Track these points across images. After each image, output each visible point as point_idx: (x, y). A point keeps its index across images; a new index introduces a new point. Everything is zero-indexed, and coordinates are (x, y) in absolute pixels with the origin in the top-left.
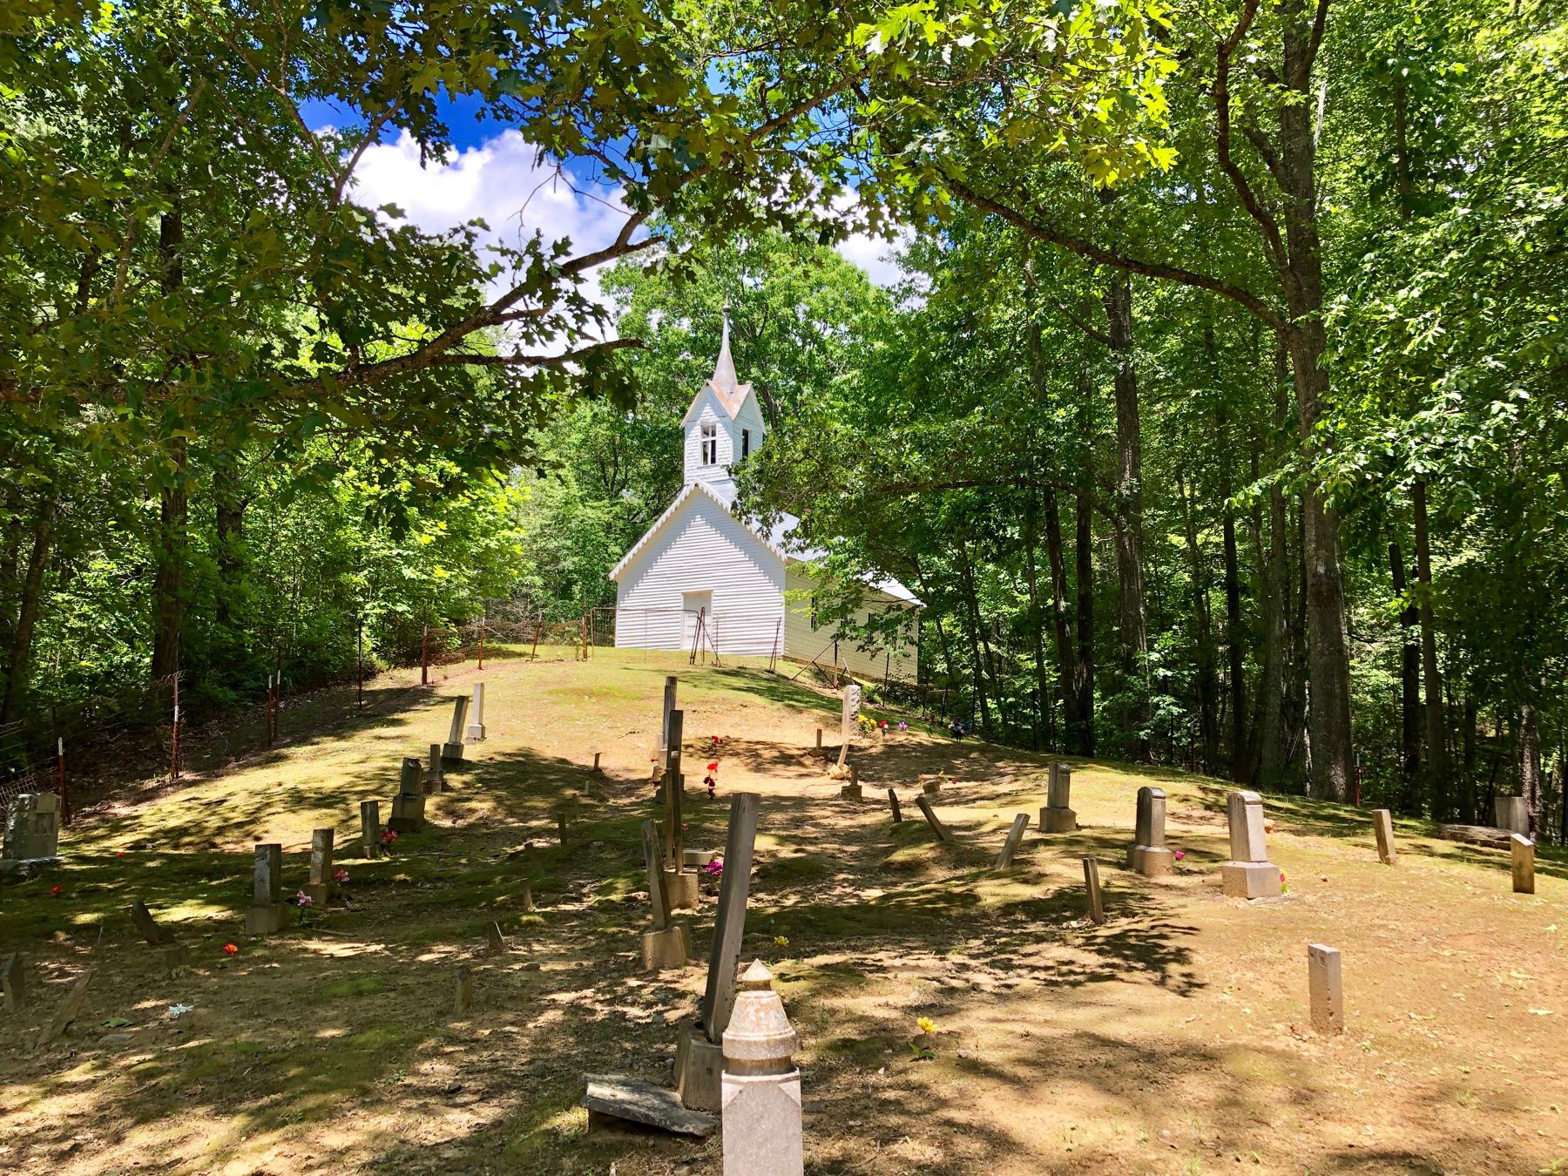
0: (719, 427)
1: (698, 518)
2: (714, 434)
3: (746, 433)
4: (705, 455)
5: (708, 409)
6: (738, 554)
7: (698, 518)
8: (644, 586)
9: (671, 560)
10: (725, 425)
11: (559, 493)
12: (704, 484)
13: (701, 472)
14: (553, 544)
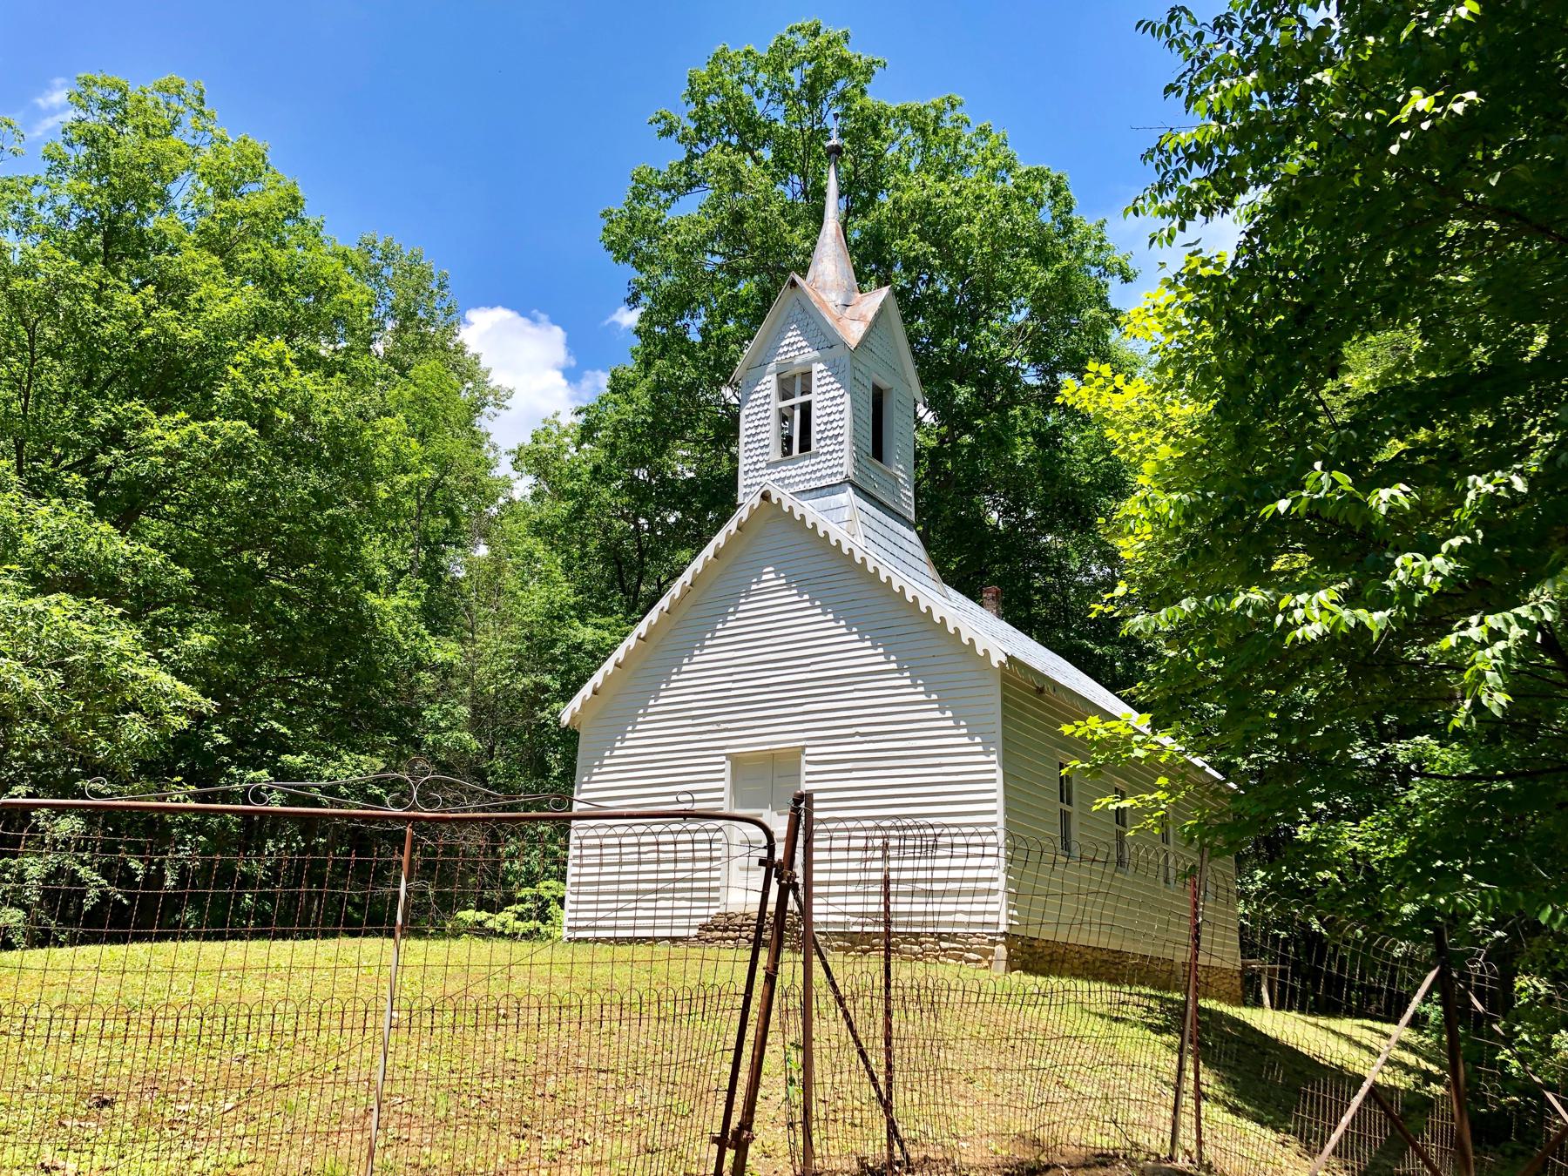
1: (769, 574)
2: (807, 390)
3: (878, 397)
4: (788, 441)
5: (793, 336)
6: (870, 657)
7: (769, 574)
8: (638, 739)
9: (707, 670)
10: (834, 368)
11: (536, 598)
12: (783, 496)
14: (526, 681)
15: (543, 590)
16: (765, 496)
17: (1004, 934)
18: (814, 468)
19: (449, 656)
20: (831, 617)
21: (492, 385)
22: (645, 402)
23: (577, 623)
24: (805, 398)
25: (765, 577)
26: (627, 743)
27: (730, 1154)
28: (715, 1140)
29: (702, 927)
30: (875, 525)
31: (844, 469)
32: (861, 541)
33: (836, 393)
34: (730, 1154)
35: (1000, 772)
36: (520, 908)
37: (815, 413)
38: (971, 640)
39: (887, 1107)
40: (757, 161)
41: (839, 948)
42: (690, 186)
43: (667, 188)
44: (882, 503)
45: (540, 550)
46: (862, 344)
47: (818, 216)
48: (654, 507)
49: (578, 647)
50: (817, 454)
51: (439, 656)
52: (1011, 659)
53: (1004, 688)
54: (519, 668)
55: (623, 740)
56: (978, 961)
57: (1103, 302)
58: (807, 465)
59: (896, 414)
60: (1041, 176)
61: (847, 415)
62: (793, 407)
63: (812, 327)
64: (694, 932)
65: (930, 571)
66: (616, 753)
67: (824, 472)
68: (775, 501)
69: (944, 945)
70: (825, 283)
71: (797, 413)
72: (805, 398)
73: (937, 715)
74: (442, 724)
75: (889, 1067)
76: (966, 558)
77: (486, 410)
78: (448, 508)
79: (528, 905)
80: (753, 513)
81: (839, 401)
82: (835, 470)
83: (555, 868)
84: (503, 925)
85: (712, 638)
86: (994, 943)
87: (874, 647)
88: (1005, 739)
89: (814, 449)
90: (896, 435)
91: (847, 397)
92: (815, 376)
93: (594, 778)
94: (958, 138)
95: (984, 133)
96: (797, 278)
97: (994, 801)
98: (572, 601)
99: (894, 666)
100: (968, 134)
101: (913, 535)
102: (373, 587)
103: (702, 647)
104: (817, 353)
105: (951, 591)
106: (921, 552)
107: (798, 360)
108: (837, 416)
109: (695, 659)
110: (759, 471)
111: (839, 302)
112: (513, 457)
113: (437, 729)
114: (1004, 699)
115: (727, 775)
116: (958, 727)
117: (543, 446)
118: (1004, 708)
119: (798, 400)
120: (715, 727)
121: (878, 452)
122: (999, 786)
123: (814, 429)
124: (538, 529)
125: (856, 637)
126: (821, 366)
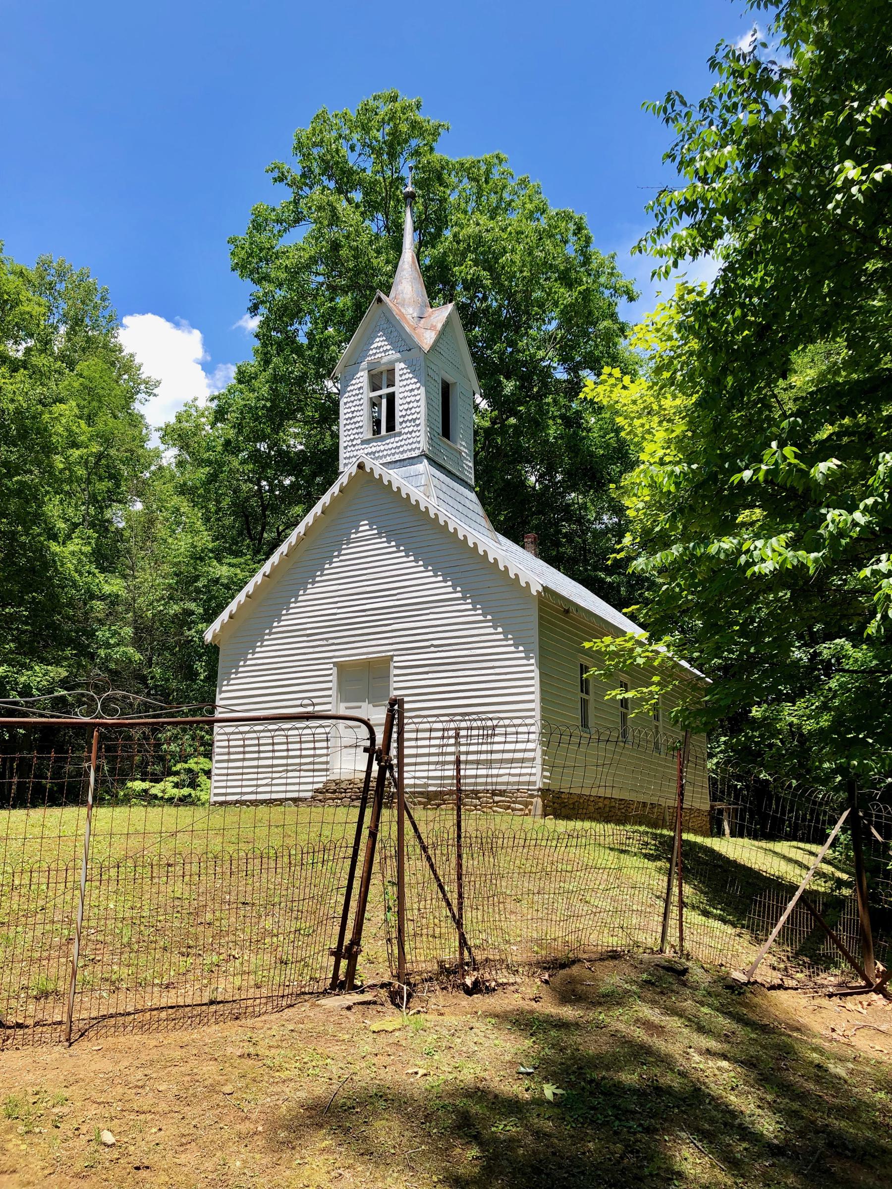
0: (400, 366)
1: (364, 525)
2: (391, 384)
3: (446, 390)
5: (380, 342)
7: (364, 525)
8: (267, 651)
9: (319, 601)
10: (412, 367)
11: (182, 544)
12: (375, 466)
13: (374, 447)
14: (175, 609)
15: (187, 536)
16: (361, 466)
17: (539, 790)
18: (396, 441)
19: (115, 589)
20: (412, 558)
21: (143, 376)
22: (265, 390)
23: (215, 563)
24: (390, 390)
25: (361, 529)
26: (256, 656)
27: (344, 963)
28: (333, 953)
29: (317, 791)
30: (445, 488)
31: (421, 445)
32: (434, 501)
33: (414, 386)
34: (344, 963)
35: (537, 672)
36: (175, 779)
37: (398, 402)
38: (516, 575)
39: (459, 924)
40: (349, 201)
41: (420, 803)
42: (297, 221)
43: (279, 221)
44: (450, 472)
45: (185, 507)
46: (434, 348)
47: (398, 247)
48: (273, 474)
49: (216, 581)
50: (400, 434)
51: (107, 589)
52: (546, 589)
53: (540, 610)
54: (171, 598)
55: (253, 653)
56: (521, 810)
57: (613, 316)
58: (393, 442)
59: (460, 402)
60: (568, 217)
61: (423, 403)
62: (380, 397)
63: (395, 334)
64: (310, 794)
65: (485, 523)
66: (249, 663)
67: (405, 448)
68: (368, 470)
69: (497, 798)
70: (404, 300)
71: (384, 401)
72: (390, 390)
73: (492, 630)
74: (112, 641)
75: (460, 896)
76: (513, 512)
77: (139, 396)
78: (112, 472)
79: (183, 776)
80: (351, 479)
81: (416, 392)
82: (414, 446)
83: (202, 748)
84: (163, 791)
85: (321, 576)
86: (532, 796)
87: (445, 581)
88: (540, 647)
89: (397, 430)
90: (460, 419)
91: (423, 389)
92: (397, 373)
93: (232, 682)
94: (504, 187)
95: (524, 183)
96: (383, 296)
97: (533, 693)
98: (210, 546)
99: (459, 595)
100: (512, 184)
101: (473, 496)
102: (54, 537)
103: (314, 583)
104: (398, 355)
105: (501, 538)
106: (479, 509)
107: (384, 360)
108: (415, 404)
109: (308, 591)
110: (355, 447)
111: (415, 315)
112: (161, 433)
113: (108, 646)
114: (541, 618)
115: (334, 678)
116: (506, 639)
117: (185, 425)
118: (540, 625)
119: (385, 391)
120: (325, 642)
121: (446, 432)
122: (536, 682)
123: (398, 414)
124: (183, 490)
125: (431, 574)
126: (402, 365)
